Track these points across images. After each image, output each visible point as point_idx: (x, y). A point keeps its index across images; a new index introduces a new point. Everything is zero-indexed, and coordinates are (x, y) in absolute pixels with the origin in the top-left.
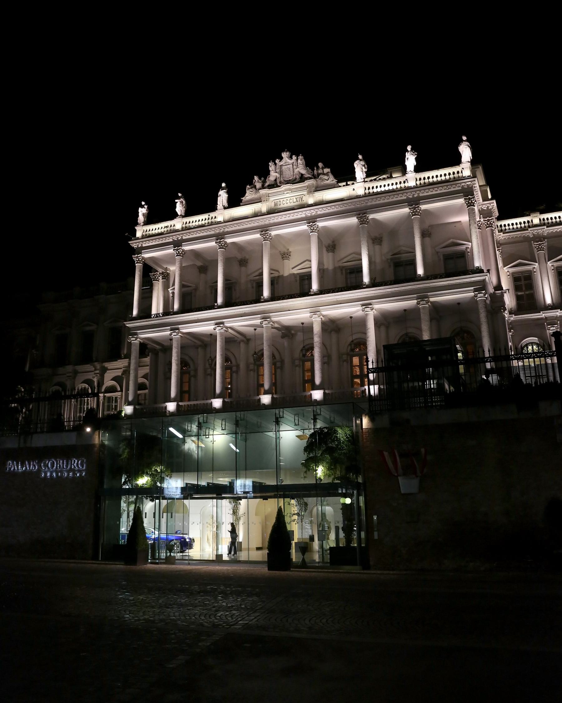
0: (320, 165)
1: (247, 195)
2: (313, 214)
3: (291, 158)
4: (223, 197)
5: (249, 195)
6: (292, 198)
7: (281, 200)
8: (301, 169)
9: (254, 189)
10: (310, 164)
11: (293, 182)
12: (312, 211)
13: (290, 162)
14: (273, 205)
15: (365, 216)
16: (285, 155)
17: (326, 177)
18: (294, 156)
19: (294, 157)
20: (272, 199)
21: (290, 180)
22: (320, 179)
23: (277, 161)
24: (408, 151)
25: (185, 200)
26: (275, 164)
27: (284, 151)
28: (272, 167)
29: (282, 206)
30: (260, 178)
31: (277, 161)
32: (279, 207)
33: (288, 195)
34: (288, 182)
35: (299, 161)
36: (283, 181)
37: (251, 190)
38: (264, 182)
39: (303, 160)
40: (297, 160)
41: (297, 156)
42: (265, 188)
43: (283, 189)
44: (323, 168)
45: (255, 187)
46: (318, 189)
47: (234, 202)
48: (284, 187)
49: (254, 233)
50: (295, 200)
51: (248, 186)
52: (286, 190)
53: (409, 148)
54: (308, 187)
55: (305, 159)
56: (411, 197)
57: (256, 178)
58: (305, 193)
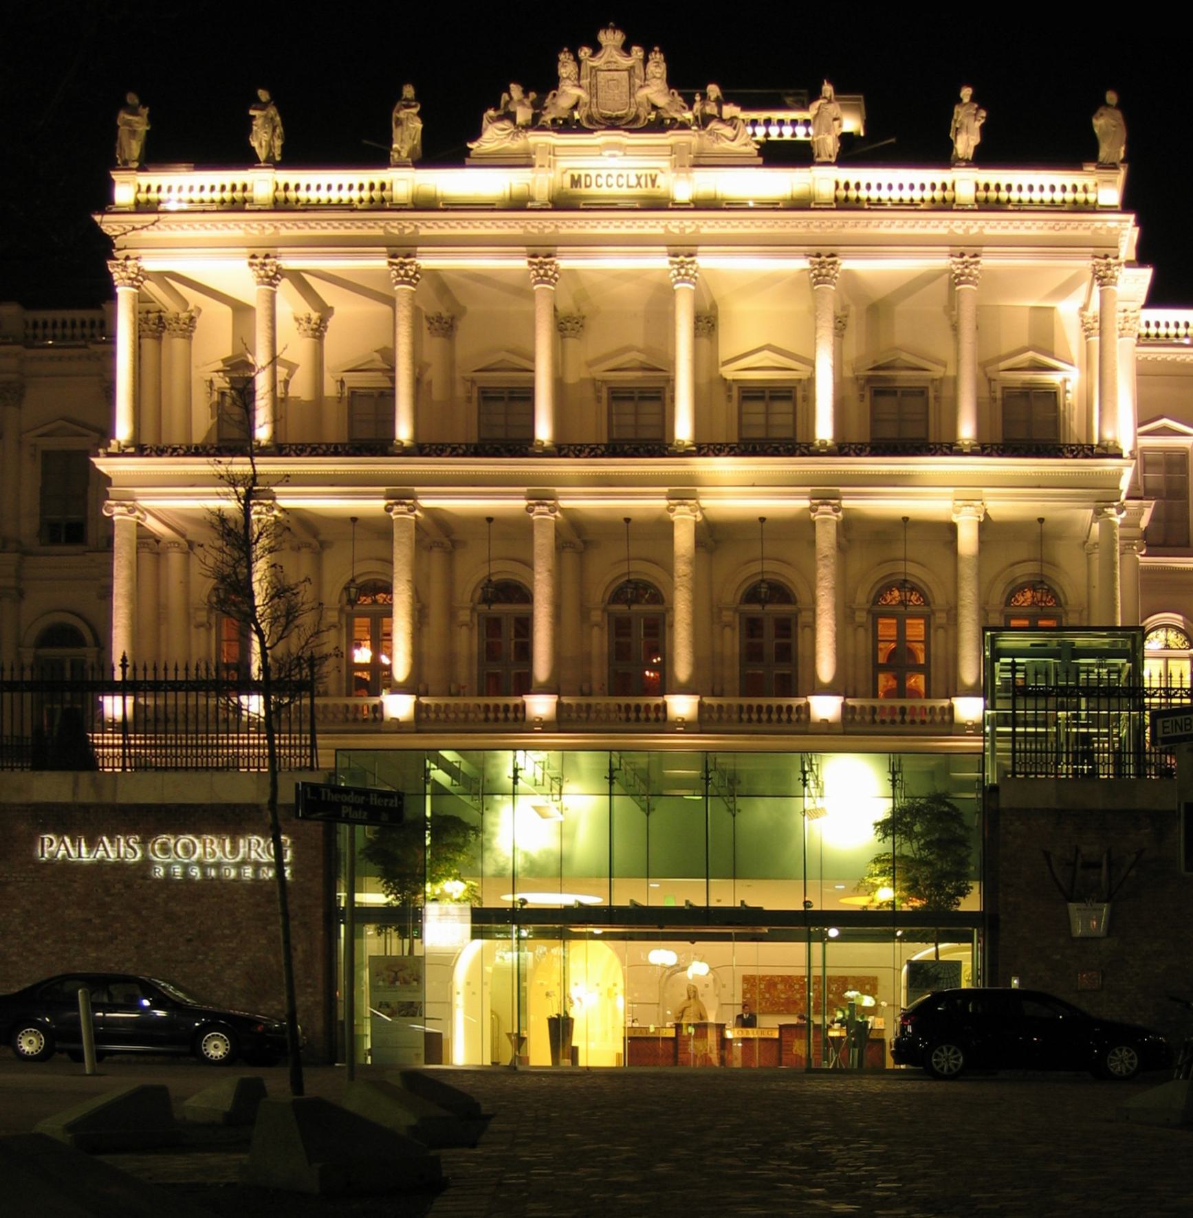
0: (713, 90)
2: (688, 231)
4: (409, 129)
5: (493, 137)
6: (624, 173)
8: (655, 91)
9: (506, 124)
10: (684, 81)
11: (630, 124)
12: (687, 223)
13: (625, 62)
15: (834, 263)
16: (611, 39)
17: (728, 131)
19: (637, 52)
20: (563, 164)
21: (618, 118)
22: (711, 133)
23: (585, 52)
24: (960, 101)
25: (281, 112)
26: (578, 61)
27: (606, 27)
28: (566, 69)
29: (593, 190)
30: (526, 93)
32: (583, 191)
34: (612, 123)
35: (651, 67)
36: (597, 116)
37: (500, 125)
38: (538, 106)
39: (663, 66)
40: (646, 61)
41: (647, 51)
42: (543, 128)
44: (719, 103)
45: (511, 116)
46: (701, 161)
47: (447, 146)
48: (601, 138)
49: (510, 256)
50: (633, 181)
51: (491, 112)
52: (609, 146)
53: (966, 93)
54: (673, 149)
55: (667, 60)
56: (960, 232)
57: (516, 91)
58: (665, 164)
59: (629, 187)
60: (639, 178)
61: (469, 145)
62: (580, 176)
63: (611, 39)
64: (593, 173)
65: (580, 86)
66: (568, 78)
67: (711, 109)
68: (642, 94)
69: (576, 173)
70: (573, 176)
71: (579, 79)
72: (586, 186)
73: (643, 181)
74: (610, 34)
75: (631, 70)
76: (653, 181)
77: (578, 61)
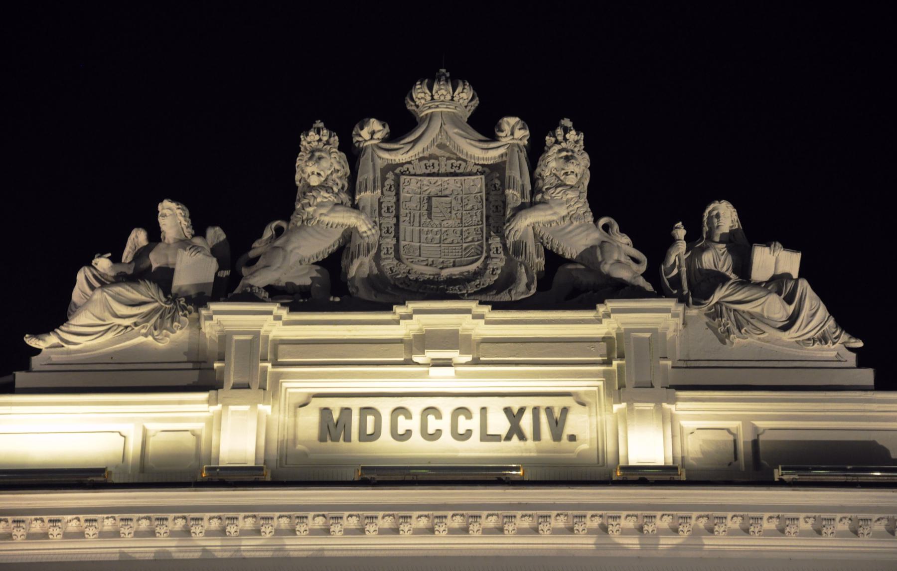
0: (725, 216)
1: (81, 320)
3: (484, 124)
6: (474, 405)
7: (385, 407)
8: (563, 216)
14: (308, 424)
16: (442, 103)
18: (510, 122)
19: (514, 131)
20: (296, 386)
23: (372, 131)
26: (352, 154)
29: (385, 447)
31: (372, 131)
32: (355, 447)
33: (441, 379)
35: (551, 163)
39: (584, 160)
40: (535, 151)
43: (403, 330)
50: (499, 424)
51: (103, 263)
54: (612, 348)
57: (172, 217)
58: (589, 384)
59: (486, 437)
60: (514, 416)
61: (32, 342)
62: (346, 411)
63: (442, 103)
64: (385, 407)
65: (355, 206)
66: (324, 187)
67: (716, 258)
68: (523, 225)
69: (336, 405)
70: (325, 412)
71: (352, 191)
72: (364, 437)
73: (526, 422)
74: (442, 90)
75: (494, 173)
76: (557, 426)
77: (352, 154)
